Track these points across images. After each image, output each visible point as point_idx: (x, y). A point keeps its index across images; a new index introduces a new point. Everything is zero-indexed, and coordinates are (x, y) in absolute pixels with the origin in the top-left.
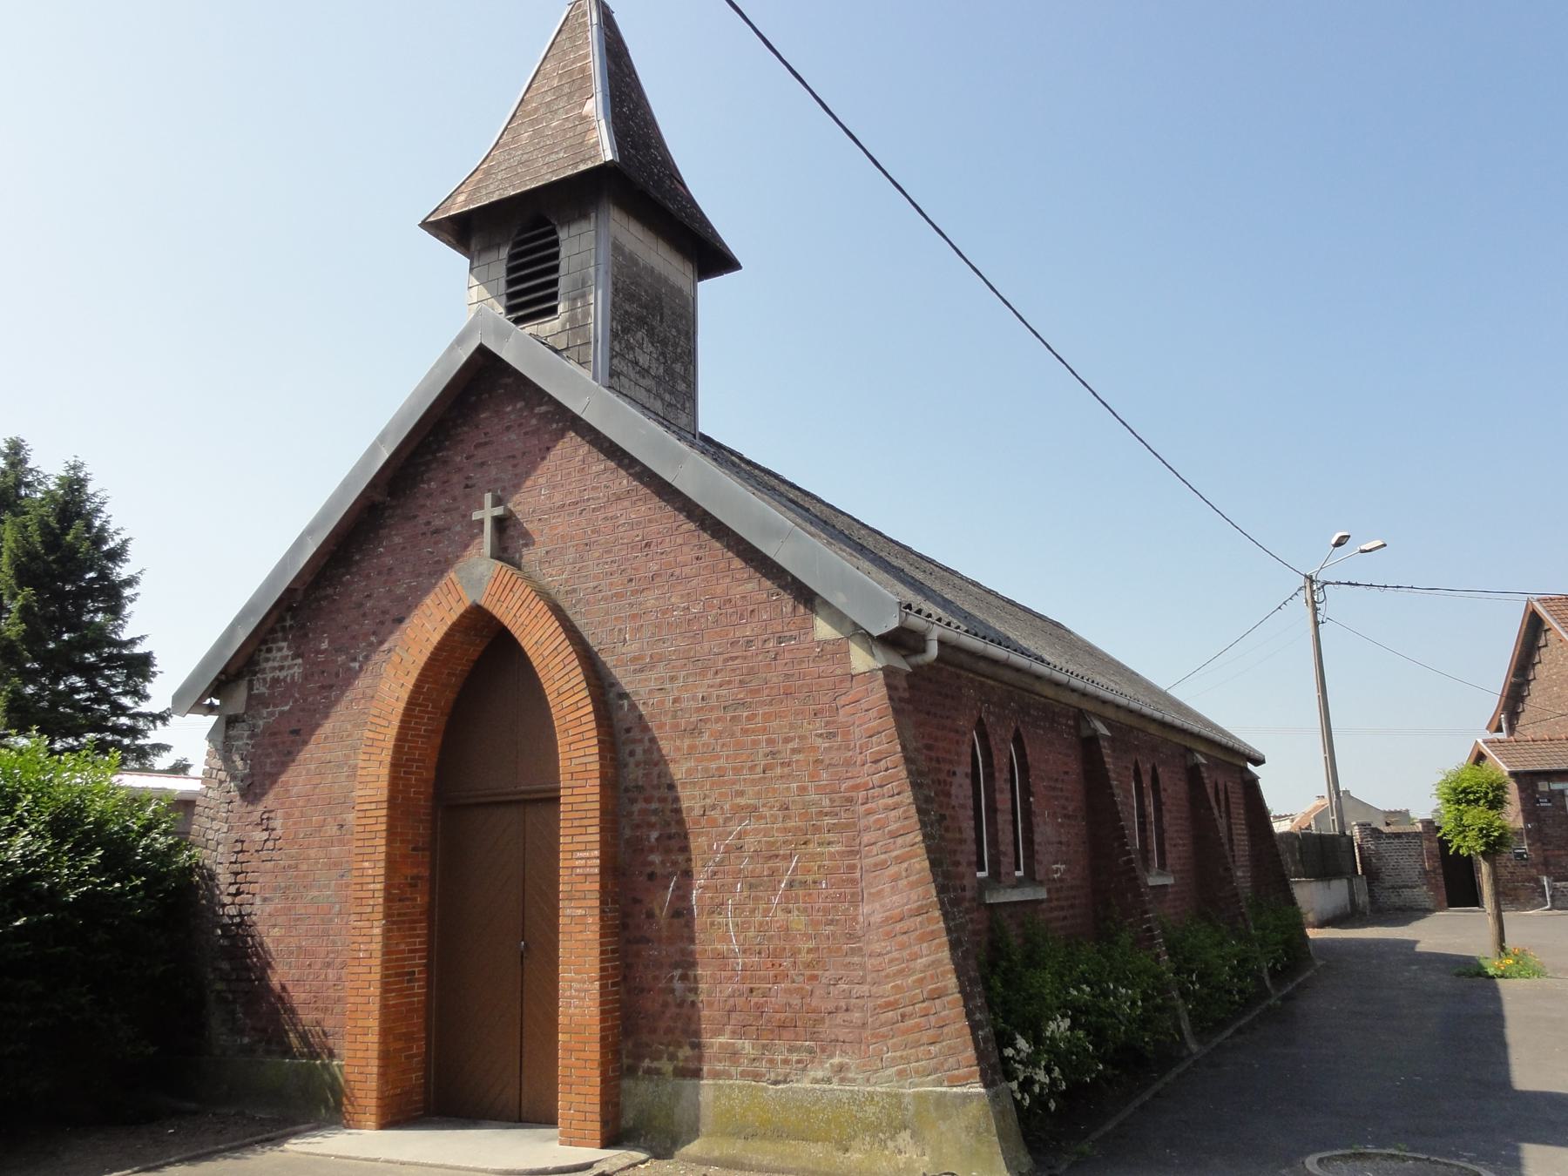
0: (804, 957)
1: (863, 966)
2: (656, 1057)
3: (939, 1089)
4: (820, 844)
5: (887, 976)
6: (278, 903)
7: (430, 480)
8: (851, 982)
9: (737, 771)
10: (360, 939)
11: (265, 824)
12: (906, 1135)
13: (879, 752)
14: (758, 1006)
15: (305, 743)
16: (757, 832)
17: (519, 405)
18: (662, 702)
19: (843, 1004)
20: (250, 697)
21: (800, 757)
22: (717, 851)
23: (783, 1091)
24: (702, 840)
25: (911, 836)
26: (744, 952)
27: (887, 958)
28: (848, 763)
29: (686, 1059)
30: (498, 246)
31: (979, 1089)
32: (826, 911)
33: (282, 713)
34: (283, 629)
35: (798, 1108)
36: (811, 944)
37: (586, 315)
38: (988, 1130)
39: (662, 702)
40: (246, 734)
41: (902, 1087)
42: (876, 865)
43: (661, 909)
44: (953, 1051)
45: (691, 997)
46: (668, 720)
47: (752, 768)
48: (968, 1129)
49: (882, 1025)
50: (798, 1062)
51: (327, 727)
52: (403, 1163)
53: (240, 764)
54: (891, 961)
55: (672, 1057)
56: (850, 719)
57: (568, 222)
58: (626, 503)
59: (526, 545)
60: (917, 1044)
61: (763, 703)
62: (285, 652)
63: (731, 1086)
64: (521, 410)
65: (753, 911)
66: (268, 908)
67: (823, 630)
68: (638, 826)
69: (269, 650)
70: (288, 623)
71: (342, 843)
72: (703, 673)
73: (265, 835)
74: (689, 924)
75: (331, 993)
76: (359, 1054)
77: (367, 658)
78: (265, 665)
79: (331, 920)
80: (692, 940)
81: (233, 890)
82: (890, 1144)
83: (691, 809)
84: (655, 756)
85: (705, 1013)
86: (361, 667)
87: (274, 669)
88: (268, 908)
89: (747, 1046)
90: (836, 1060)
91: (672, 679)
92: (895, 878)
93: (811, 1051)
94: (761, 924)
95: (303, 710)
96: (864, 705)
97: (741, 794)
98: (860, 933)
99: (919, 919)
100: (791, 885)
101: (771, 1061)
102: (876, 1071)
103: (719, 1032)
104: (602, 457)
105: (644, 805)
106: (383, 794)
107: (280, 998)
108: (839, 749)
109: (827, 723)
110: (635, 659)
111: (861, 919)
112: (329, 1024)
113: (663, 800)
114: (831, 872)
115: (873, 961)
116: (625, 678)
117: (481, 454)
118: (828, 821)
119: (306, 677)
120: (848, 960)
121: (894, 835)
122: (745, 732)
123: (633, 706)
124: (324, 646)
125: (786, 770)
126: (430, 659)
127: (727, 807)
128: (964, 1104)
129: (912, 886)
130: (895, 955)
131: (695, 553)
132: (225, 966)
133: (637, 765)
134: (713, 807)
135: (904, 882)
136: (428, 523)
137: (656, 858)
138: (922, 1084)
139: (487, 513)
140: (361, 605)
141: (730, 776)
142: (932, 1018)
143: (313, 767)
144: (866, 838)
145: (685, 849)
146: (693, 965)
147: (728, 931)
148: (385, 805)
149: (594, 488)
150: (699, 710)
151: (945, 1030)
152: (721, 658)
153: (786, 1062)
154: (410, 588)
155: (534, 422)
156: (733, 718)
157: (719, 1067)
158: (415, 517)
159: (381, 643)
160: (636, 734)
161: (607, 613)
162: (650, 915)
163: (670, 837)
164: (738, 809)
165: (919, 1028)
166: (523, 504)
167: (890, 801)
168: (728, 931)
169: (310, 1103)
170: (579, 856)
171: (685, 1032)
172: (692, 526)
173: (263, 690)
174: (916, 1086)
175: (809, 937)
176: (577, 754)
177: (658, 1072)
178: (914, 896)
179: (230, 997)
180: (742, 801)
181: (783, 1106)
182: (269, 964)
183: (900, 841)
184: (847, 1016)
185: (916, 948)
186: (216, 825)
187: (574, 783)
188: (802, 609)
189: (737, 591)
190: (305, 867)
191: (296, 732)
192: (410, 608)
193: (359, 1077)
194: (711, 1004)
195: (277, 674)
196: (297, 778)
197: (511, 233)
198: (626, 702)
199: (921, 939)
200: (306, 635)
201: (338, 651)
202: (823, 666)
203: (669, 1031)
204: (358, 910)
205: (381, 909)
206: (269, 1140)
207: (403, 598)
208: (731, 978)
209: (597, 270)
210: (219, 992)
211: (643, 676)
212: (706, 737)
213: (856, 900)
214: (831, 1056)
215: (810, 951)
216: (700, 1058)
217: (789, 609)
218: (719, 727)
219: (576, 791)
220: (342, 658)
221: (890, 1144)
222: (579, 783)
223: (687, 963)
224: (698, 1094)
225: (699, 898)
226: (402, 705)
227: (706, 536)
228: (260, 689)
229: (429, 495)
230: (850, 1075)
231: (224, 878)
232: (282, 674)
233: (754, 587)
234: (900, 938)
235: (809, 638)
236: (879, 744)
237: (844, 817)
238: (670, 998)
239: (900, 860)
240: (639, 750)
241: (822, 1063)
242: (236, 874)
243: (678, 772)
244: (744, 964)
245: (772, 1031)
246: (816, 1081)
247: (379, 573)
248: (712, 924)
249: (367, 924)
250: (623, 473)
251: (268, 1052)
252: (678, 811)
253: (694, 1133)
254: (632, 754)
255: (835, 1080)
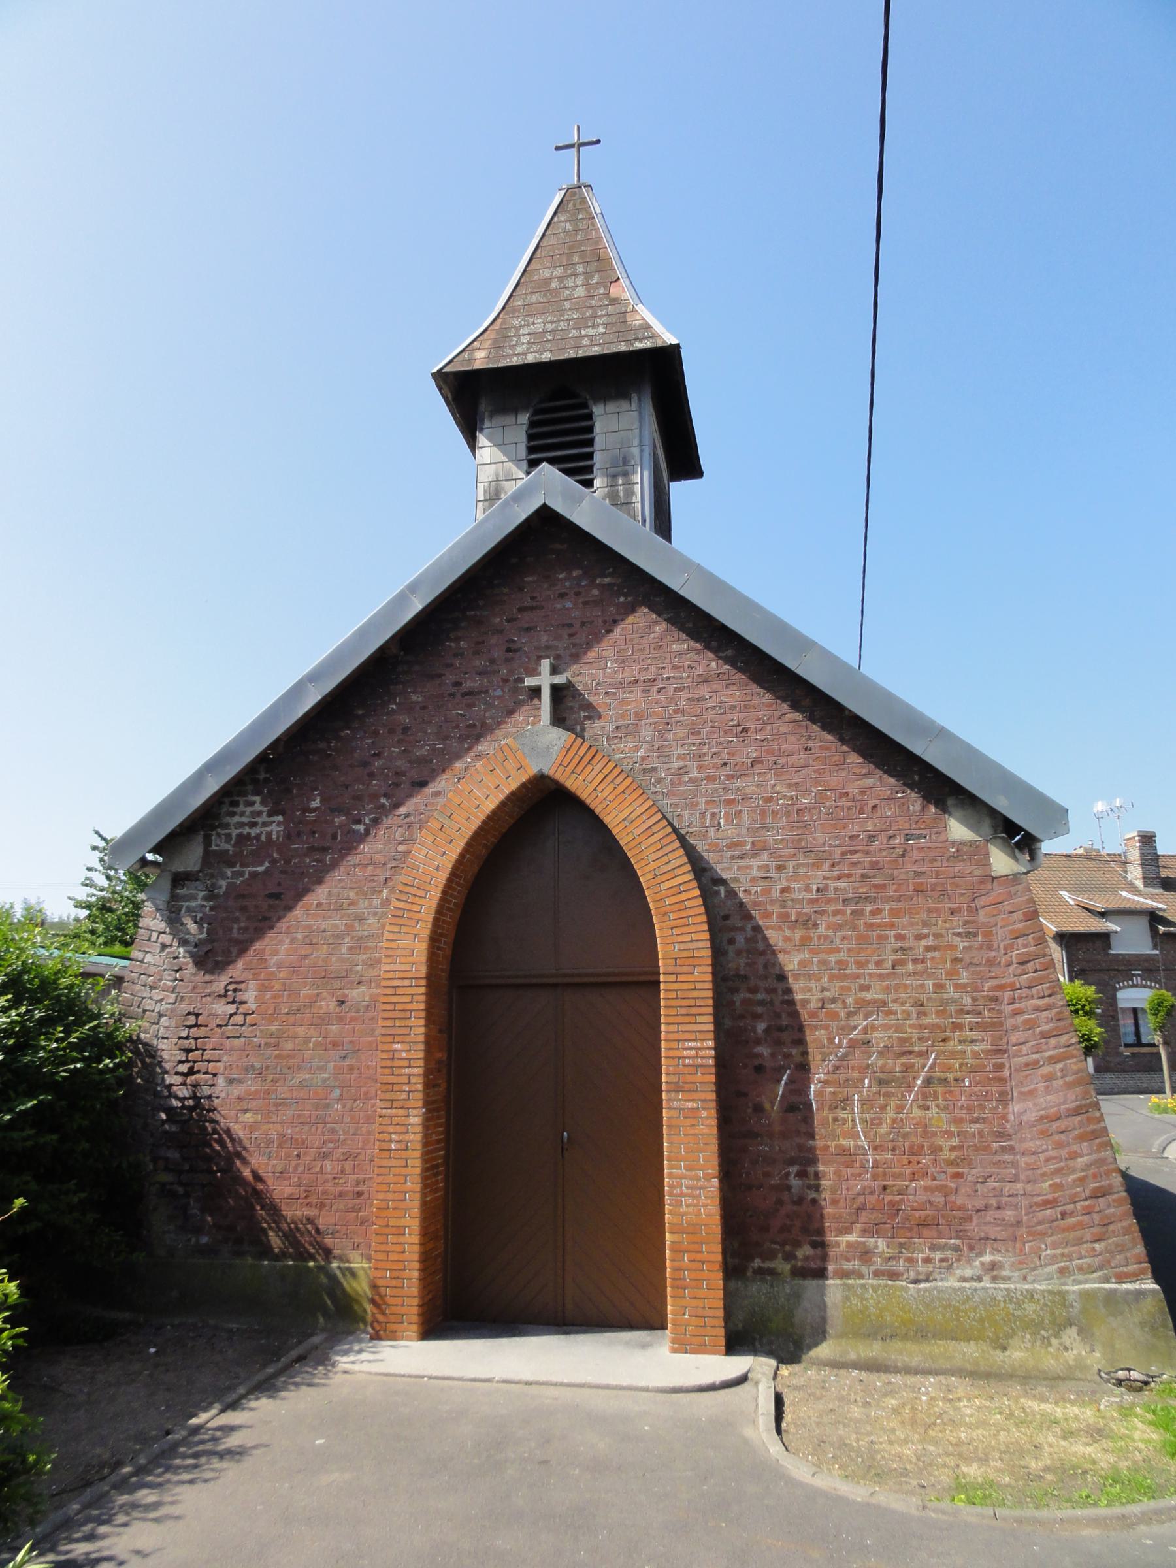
0: (946, 1154)
1: (1014, 1164)
2: (771, 1256)
3: (1107, 1286)
4: (960, 1042)
5: (1044, 1175)
6: (251, 1085)
7: (457, 640)
8: (1003, 1180)
9: (860, 965)
10: (391, 1129)
11: (232, 995)
12: (1072, 1332)
13: (1027, 954)
14: (892, 1204)
15: (289, 908)
16: (886, 1027)
17: (575, 574)
18: (767, 892)
19: (993, 1202)
20: (207, 854)
21: (936, 954)
22: (840, 1045)
23: (926, 1290)
24: (821, 1034)
25: (1065, 1037)
26: (875, 1148)
27: (1042, 1157)
28: (991, 962)
29: (807, 1258)
30: (516, 411)
31: (1151, 1285)
32: (970, 1109)
33: (254, 875)
34: (255, 781)
35: (945, 1307)
36: (955, 1142)
37: (631, 493)
38: (1165, 1326)
39: (767, 892)
40: (201, 894)
41: (1065, 1284)
42: (1027, 1065)
43: (773, 1104)
44: (1122, 1249)
45: (812, 1195)
46: (775, 910)
47: (879, 964)
48: (1142, 1324)
49: (1039, 1223)
50: (942, 1260)
51: (321, 893)
52: (528, 1383)
53: (192, 927)
54: (1047, 1160)
55: (789, 1257)
56: (992, 920)
57: (604, 398)
58: (715, 686)
59: (589, 718)
60: (1080, 1242)
61: (888, 899)
62: (258, 807)
63: (863, 1286)
64: (579, 578)
65: (883, 1108)
66: (236, 1091)
67: (958, 830)
68: (742, 1017)
69: (236, 804)
70: (262, 776)
71: (341, 1020)
72: (818, 863)
73: (231, 1009)
74: (808, 1118)
75: (329, 1187)
76: (392, 1257)
77: (376, 822)
78: (228, 819)
79: (327, 1106)
80: (812, 1136)
81: (183, 1068)
82: (1054, 1341)
83: (807, 1001)
84: (761, 946)
85: (829, 1210)
86: (367, 832)
87: (242, 825)
88: (236, 1091)
89: (881, 1245)
90: (987, 1258)
91: (780, 868)
92: (1049, 1078)
93: (956, 1249)
94: (894, 1121)
95: (284, 872)
96: (1007, 906)
97: (866, 988)
98: (1011, 1131)
99: (1078, 1118)
100: (928, 1081)
101: (910, 1260)
102: (1034, 1269)
103: (848, 1231)
104: (685, 637)
105: (748, 995)
106: (423, 970)
107: (257, 1193)
108: (981, 948)
109: (966, 923)
110: (730, 846)
111: (1011, 1117)
112: (325, 1221)
113: (774, 991)
114: (974, 1069)
115: (1026, 1159)
116: (722, 867)
117: (526, 619)
118: (969, 1019)
119: (288, 836)
120: (997, 1158)
121: (1046, 1036)
122: (870, 926)
123: (732, 894)
124: (316, 803)
125: (919, 967)
126: (480, 828)
127: (850, 1001)
128: (1137, 1300)
129: (1069, 1086)
130: (1051, 1153)
131: (803, 743)
132: (174, 1155)
133: (739, 953)
134: (833, 1000)
135: (1060, 1082)
136: (458, 684)
137: (764, 1050)
138: (1086, 1282)
139: (545, 679)
140: (365, 764)
141: (852, 969)
142: (1096, 1217)
143: (299, 936)
144: (1014, 1038)
145: (801, 1042)
146: (814, 1161)
147: (855, 1126)
148: (423, 982)
149: (674, 667)
150: (812, 902)
151: (1111, 1228)
152: (838, 851)
153: (927, 1260)
154: (433, 749)
155: (595, 592)
156: (853, 912)
157: (848, 1266)
158: (440, 675)
159: (396, 806)
160: (735, 921)
161: (695, 796)
162: (759, 1109)
163: (781, 1029)
164: (861, 1004)
165: (1080, 1226)
166: (584, 676)
167: (1040, 1002)
168: (853, 1131)
169: (289, 1314)
170: (687, 1047)
171: (805, 1230)
172: (799, 716)
173: (225, 846)
174: (1080, 1283)
175: (950, 1134)
176: (680, 939)
177: (772, 1272)
178: (1071, 1095)
179: (181, 1190)
180: (868, 996)
181: (927, 1306)
182: (239, 1155)
183: (1053, 1041)
184: (998, 1214)
185: (1075, 1148)
186: (157, 995)
187: (678, 969)
188: (933, 809)
189: (855, 787)
190: (290, 1046)
191: (277, 896)
192: (434, 774)
193: (394, 1283)
194: (835, 1202)
195: (246, 830)
196: (279, 946)
197: (536, 399)
198: (722, 889)
199: (1081, 1138)
200: (288, 791)
201: (338, 810)
202: (957, 868)
203: (784, 1229)
204: (388, 1096)
205: (420, 1096)
206: (301, 1359)
207: (424, 761)
208: (860, 1175)
209: (642, 451)
210: (163, 1185)
211: (743, 863)
212: (822, 929)
213: (1004, 1098)
214: (980, 1254)
215: (953, 1148)
216: (824, 1258)
217: (918, 807)
218: (838, 919)
219: (680, 978)
220: (339, 820)
221: (1054, 1341)
222: (685, 969)
223: (806, 1160)
224: (823, 1295)
225: (819, 1093)
226: (443, 876)
227: (816, 728)
228: (220, 844)
229: (459, 654)
230: (1004, 1273)
231: (169, 1053)
232: (254, 832)
233: (873, 784)
234: (1057, 1137)
235: (942, 837)
236: (1026, 946)
237: (987, 1016)
238: (785, 1196)
239: (1053, 1060)
240: (740, 939)
241: (969, 1262)
242: (188, 1051)
243: (790, 962)
244: (875, 1161)
245: (910, 1229)
246: (964, 1280)
247: (392, 731)
248: (835, 1120)
249: (401, 1112)
250: (711, 655)
251: (239, 1254)
252: (792, 1003)
253: (820, 1335)
254: (731, 941)
255: (986, 1278)
